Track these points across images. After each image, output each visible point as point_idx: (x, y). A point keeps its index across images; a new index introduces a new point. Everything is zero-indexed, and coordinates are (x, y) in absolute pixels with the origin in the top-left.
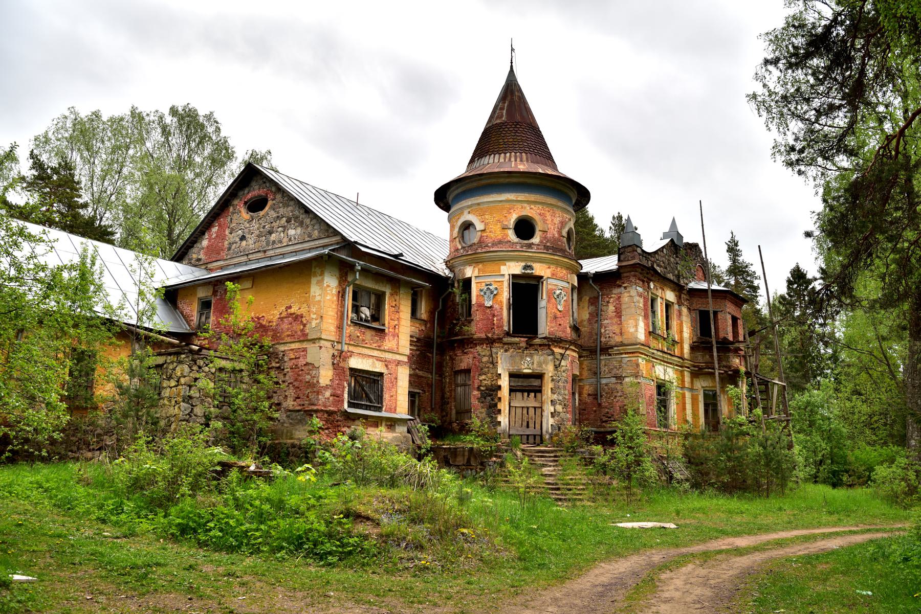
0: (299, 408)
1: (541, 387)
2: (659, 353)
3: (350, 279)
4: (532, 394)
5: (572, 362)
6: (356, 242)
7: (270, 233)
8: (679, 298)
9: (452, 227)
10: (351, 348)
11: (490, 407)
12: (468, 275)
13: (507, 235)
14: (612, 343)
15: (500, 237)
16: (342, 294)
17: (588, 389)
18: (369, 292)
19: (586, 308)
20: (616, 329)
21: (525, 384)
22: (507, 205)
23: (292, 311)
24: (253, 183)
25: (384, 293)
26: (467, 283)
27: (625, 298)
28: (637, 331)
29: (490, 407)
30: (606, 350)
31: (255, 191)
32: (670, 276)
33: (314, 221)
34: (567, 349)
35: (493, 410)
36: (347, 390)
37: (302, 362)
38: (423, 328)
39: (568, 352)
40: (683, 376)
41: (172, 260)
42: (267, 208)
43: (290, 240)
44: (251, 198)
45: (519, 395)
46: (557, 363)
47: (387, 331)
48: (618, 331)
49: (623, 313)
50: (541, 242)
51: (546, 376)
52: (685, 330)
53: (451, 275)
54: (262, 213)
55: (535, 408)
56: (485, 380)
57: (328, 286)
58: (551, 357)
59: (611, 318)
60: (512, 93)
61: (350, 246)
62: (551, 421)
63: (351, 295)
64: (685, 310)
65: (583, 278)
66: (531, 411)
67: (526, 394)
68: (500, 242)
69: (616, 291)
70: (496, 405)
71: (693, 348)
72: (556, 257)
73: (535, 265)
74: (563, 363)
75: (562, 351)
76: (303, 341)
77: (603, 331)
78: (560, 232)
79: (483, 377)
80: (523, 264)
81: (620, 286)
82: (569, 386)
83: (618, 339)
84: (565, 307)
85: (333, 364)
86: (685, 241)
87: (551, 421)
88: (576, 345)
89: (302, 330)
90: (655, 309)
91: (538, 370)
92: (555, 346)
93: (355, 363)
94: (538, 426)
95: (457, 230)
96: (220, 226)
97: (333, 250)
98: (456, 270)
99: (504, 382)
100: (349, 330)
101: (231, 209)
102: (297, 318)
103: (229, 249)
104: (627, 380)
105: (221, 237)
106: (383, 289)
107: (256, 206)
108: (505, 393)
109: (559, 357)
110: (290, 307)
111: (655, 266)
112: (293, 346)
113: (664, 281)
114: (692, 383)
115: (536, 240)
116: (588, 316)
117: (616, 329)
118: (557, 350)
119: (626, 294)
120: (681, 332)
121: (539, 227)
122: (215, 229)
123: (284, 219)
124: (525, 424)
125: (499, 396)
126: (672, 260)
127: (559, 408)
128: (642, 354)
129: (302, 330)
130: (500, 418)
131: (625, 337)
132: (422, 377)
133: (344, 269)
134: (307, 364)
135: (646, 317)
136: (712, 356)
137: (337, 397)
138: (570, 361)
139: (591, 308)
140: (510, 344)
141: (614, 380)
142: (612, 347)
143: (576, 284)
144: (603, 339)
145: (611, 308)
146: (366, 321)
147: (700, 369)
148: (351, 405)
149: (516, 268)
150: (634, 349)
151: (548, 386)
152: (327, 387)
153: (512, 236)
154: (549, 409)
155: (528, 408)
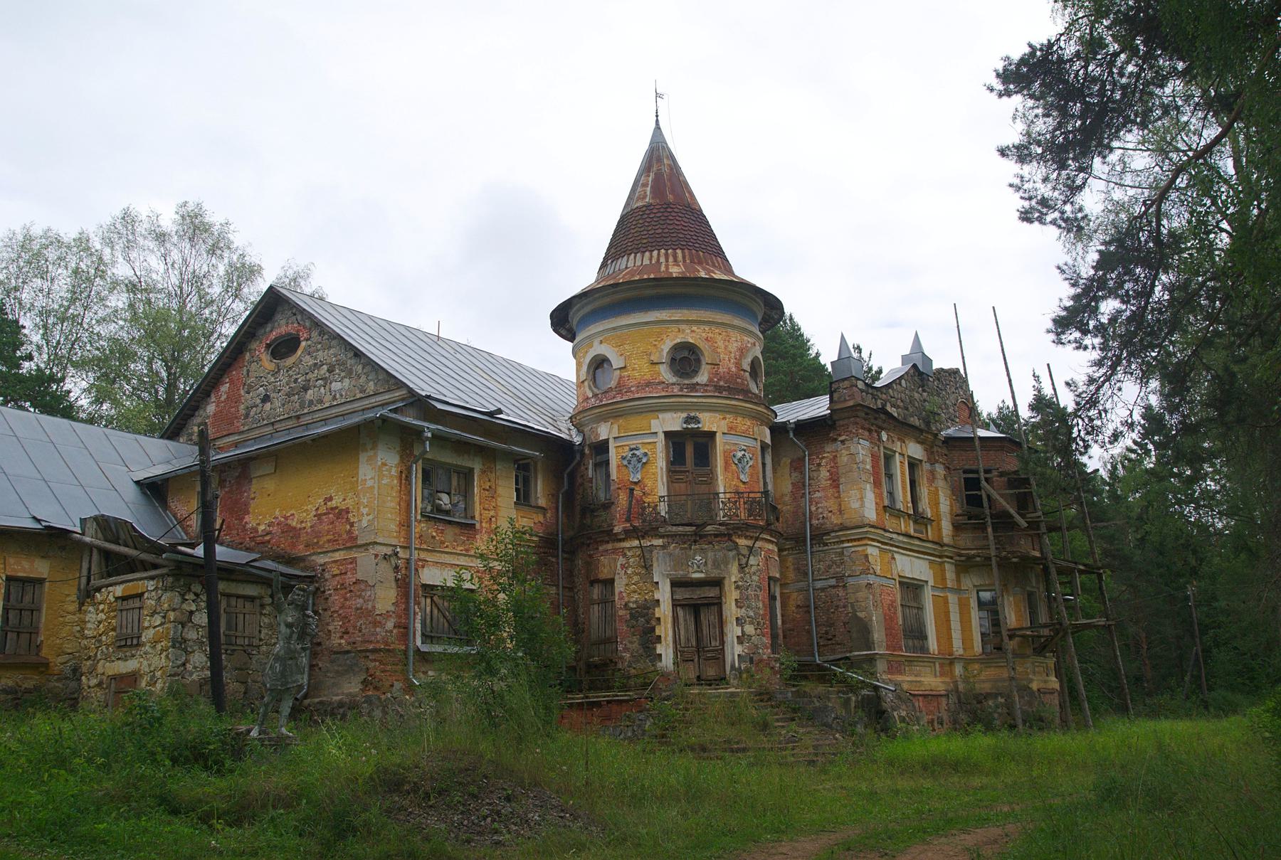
0: (349, 648)
1: (720, 598)
2: (901, 538)
3: (416, 453)
5: (767, 559)
6: (429, 397)
7: (306, 389)
8: (929, 451)
9: (579, 365)
10: (423, 555)
11: (645, 633)
12: (603, 437)
13: (659, 374)
14: (828, 526)
15: (648, 377)
16: (405, 477)
17: (796, 599)
18: (449, 469)
19: (787, 476)
20: (831, 504)
22: (656, 328)
23: (333, 504)
24: (278, 317)
25: (471, 470)
26: (602, 447)
28: (862, 506)
29: (645, 633)
30: (820, 536)
31: (282, 327)
32: (915, 421)
33: (368, 368)
34: (757, 539)
35: (649, 638)
36: (419, 617)
37: (350, 578)
38: (541, 519)
39: (758, 544)
40: (943, 571)
41: (162, 437)
42: (299, 352)
43: (335, 398)
44: (276, 339)
46: (744, 561)
47: (478, 526)
48: (835, 508)
49: (842, 480)
50: (710, 380)
51: (726, 582)
52: (941, 502)
53: (577, 440)
54: (290, 361)
57: (384, 464)
58: (734, 552)
60: (659, 160)
61: (421, 404)
62: (738, 650)
63: (420, 475)
64: (940, 470)
65: (779, 430)
68: (648, 384)
69: (829, 448)
70: (653, 629)
71: (957, 527)
72: (733, 402)
74: (752, 561)
75: (750, 543)
76: (350, 548)
77: (813, 509)
78: (738, 365)
80: (685, 415)
81: (835, 440)
82: (763, 595)
83: (836, 520)
84: (751, 475)
85: (397, 580)
86: (935, 366)
87: (738, 650)
88: (771, 533)
89: (349, 532)
90: (893, 471)
91: (715, 574)
92: (739, 537)
93: (431, 576)
95: (585, 368)
96: (232, 382)
97: (395, 411)
98: (586, 430)
100: (419, 527)
101: (247, 356)
102: (342, 514)
103: (247, 416)
105: (234, 399)
106: (469, 465)
109: (745, 552)
110: (331, 499)
111: (888, 408)
112: (338, 556)
113: (903, 428)
114: (958, 580)
115: (702, 378)
116: (790, 487)
117: (831, 504)
118: (742, 542)
120: (935, 504)
121: (707, 357)
122: (225, 388)
126: (916, 395)
127: (750, 629)
128: (873, 540)
129: (349, 532)
130: (660, 649)
133: (407, 438)
134: (357, 582)
135: (877, 484)
136: (986, 538)
137: (404, 630)
138: (764, 556)
139: (794, 475)
140: (672, 536)
142: (828, 534)
143: (768, 441)
144: (815, 522)
145: (824, 473)
146: (447, 513)
147: (969, 558)
148: (426, 638)
149: (674, 422)
150: (857, 531)
151: (731, 595)
152: (387, 615)
153: (666, 374)
154: (733, 631)
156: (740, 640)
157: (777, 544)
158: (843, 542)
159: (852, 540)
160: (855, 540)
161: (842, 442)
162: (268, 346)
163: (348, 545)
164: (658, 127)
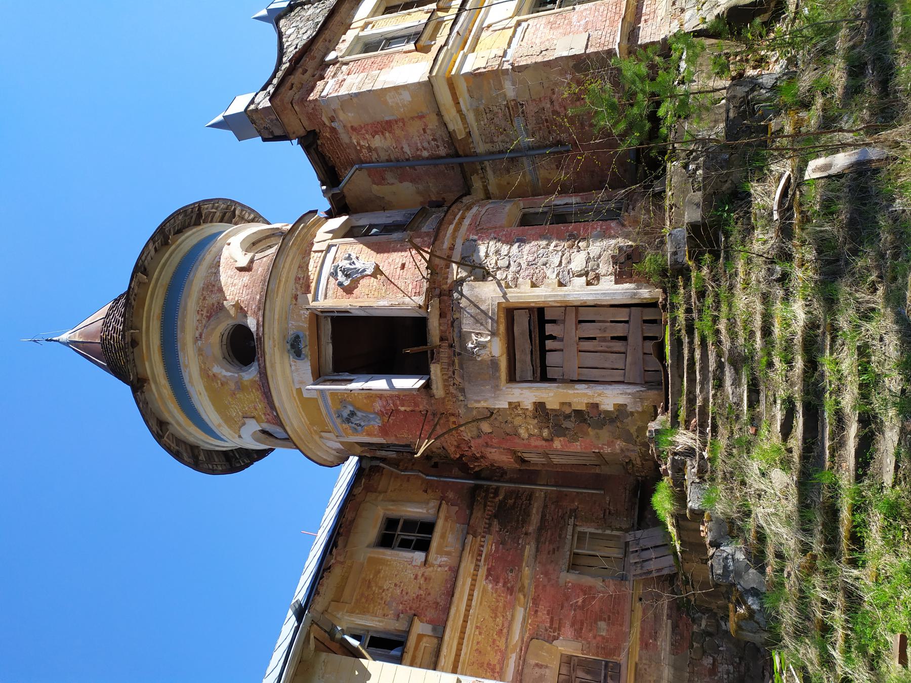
4: (550, 329)
20: (414, 129)
21: (528, 347)
35: (590, 417)
45: (551, 358)
56: (527, 429)
59: (398, 140)
66: (588, 330)
67: (549, 344)
69: (344, 138)
70: (578, 412)
77: (425, 154)
81: (333, 130)
83: (432, 122)
99: (527, 395)
108: (551, 395)
119: (342, 116)
124: (618, 346)
125: (557, 407)
131: (425, 110)
132: (543, 518)
141: (519, 123)
143: (336, 223)
145: (377, 142)
156: (593, 279)
157: (469, 208)
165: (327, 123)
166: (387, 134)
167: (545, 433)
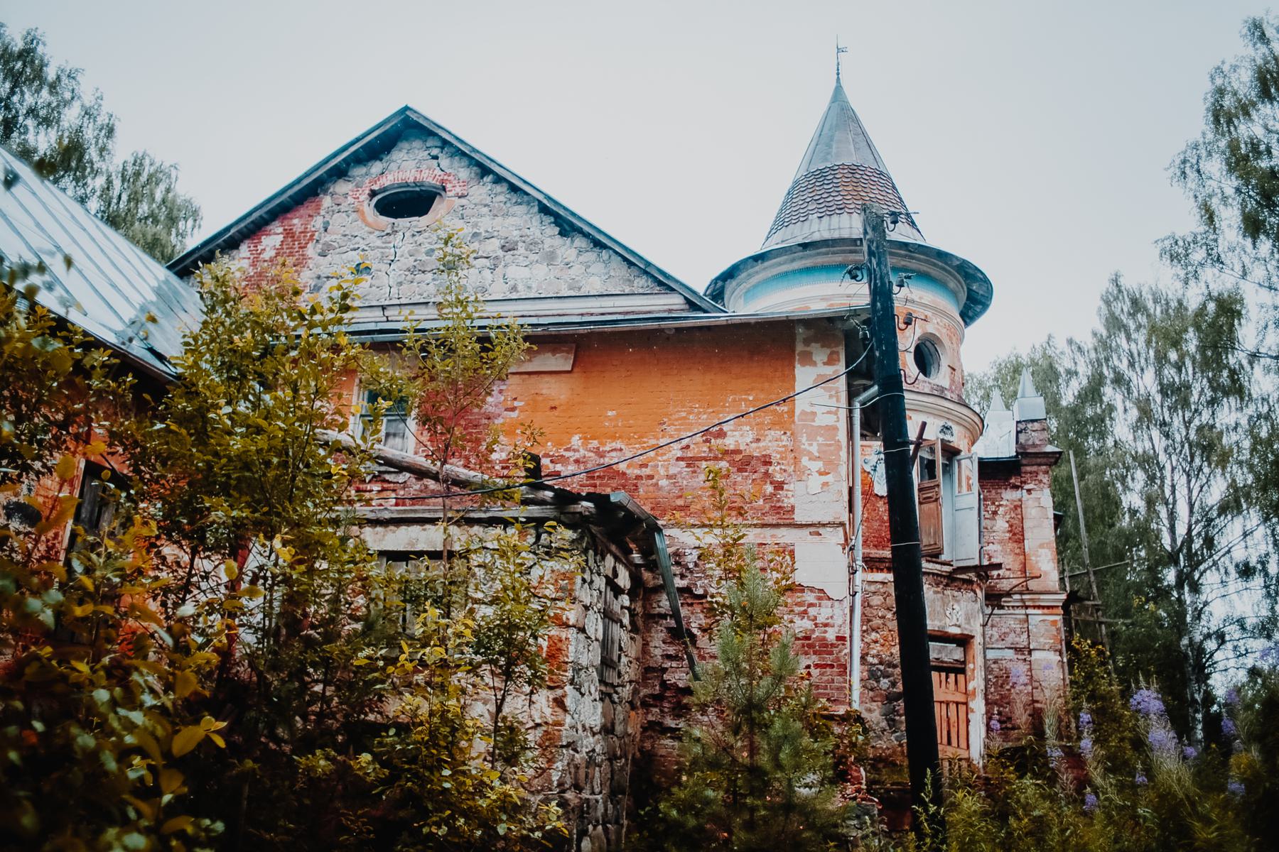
1: (964, 663)
4: (952, 676)
27: (1031, 511)
31: (407, 167)
44: (392, 187)
54: (422, 221)
55: (957, 703)
67: (943, 674)
69: (1009, 496)
73: (955, 428)
76: (777, 526)
79: (874, 636)
81: (1016, 487)
94: (963, 745)
96: (289, 234)
104: (1036, 655)
107: (407, 203)
123: (496, 243)
141: (1010, 654)
142: (1009, 594)
155: (948, 704)
158: (1027, 607)
159: (1039, 607)
160: (1043, 607)
161: (1029, 491)
162: (373, 194)
163: (770, 519)
164: (839, 89)
165: (1027, 487)
166: (1008, 535)
167: (870, 659)
